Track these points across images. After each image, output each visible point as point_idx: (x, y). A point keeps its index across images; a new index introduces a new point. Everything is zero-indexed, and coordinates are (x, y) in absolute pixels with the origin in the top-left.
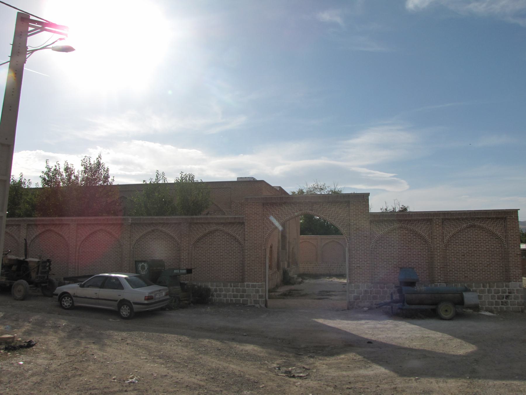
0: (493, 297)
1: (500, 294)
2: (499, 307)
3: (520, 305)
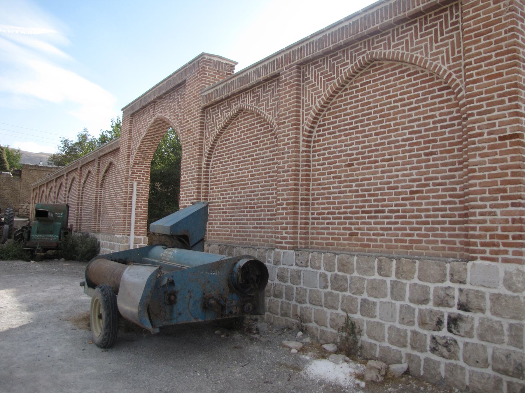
0: (406, 316)
1: (430, 306)
2: (423, 356)
3: (506, 372)
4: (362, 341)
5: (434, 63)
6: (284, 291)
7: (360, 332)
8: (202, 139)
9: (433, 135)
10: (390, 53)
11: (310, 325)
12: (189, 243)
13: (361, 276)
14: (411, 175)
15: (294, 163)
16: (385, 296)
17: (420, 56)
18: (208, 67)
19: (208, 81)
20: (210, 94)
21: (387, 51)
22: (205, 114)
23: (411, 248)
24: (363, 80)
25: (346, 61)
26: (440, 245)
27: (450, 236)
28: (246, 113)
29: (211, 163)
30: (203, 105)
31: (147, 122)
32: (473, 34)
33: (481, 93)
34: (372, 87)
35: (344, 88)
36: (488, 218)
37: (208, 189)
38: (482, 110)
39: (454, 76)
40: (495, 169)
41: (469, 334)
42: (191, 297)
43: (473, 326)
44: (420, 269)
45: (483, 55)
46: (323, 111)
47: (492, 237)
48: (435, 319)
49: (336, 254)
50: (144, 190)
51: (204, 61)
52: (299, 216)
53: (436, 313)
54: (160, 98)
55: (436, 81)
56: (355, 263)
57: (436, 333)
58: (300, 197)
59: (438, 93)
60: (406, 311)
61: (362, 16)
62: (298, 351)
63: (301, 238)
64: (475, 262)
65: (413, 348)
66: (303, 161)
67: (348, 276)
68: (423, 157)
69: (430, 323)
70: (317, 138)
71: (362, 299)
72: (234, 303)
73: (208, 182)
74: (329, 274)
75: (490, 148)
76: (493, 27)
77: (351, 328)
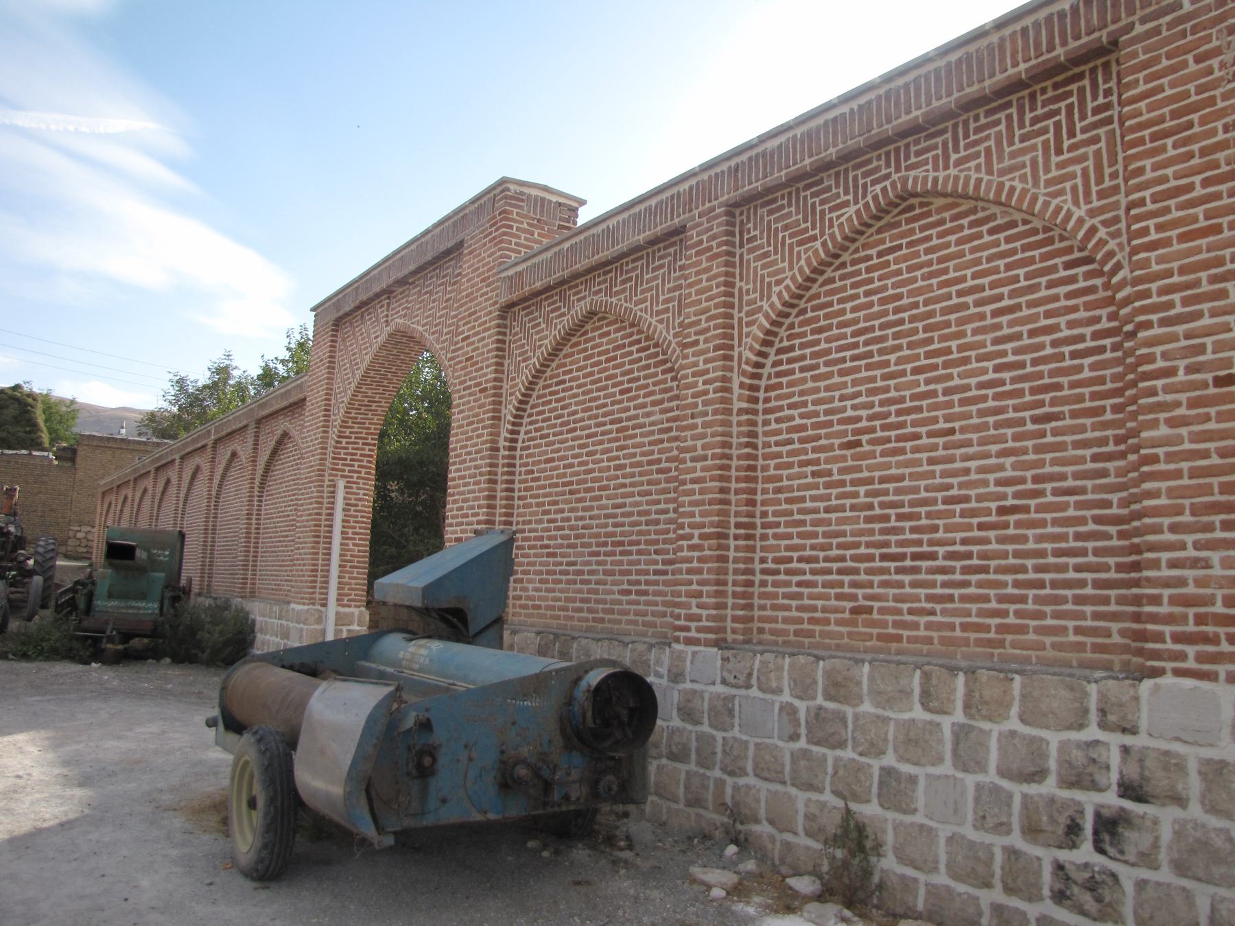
1: (1049, 787)
4: (882, 871)
5: (1055, 202)
6: (694, 745)
7: (878, 847)
8: (501, 380)
9: (1052, 374)
10: (947, 178)
11: (756, 828)
12: (465, 624)
13: (880, 712)
14: (1001, 468)
15: (719, 438)
16: (940, 760)
17: (1019, 186)
18: (515, 211)
19: (516, 244)
20: (519, 274)
21: (941, 175)
22: (508, 322)
23: (1001, 644)
24: (883, 241)
25: (843, 198)
26: (1072, 638)
27: (1097, 616)
28: (603, 318)
29: (521, 437)
30: (503, 300)
31: (371, 337)
32: (1146, 133)
33: (1168, 274)
34: (905, 258)
35: (837, 262)
36: (1189, 574)
37: (512, 498)
38: (1172, 312)
39: (1102, 233)
40: (1205, 454)
41: (1148, 859)
42: (470, 759)
43: (1157, 838)
44: (1024, 697)
45: (1173, 183)
46: (787, 315)
47: (1200, 620)
48: (1063, 820)
49: (818, 658)
50: (360, 500)
51: (506, 197)
52: (731, 566)
53: (1065, 805)
54: (402, 282)
55: (1058, 245)
56: (865, 680)
57: (1064, 855)
58: (733, 520)
59: (1063, 273)
60: (991, 797)
61: (882, 91)
62: (728, 893)
63: (735, 619)
64: (1158, 680)
65: (1008, 890)
66: (740, 435)
67: (849, 711)
68: (1030, 426)
69: (1049, 828)
70: (774, 381)
71: (882, 769)
72: (575, 775)
73: (513, 482)
74: (802, 706)
75: (1192, 404)
76: (1195, 117)
77: (855, 838)
